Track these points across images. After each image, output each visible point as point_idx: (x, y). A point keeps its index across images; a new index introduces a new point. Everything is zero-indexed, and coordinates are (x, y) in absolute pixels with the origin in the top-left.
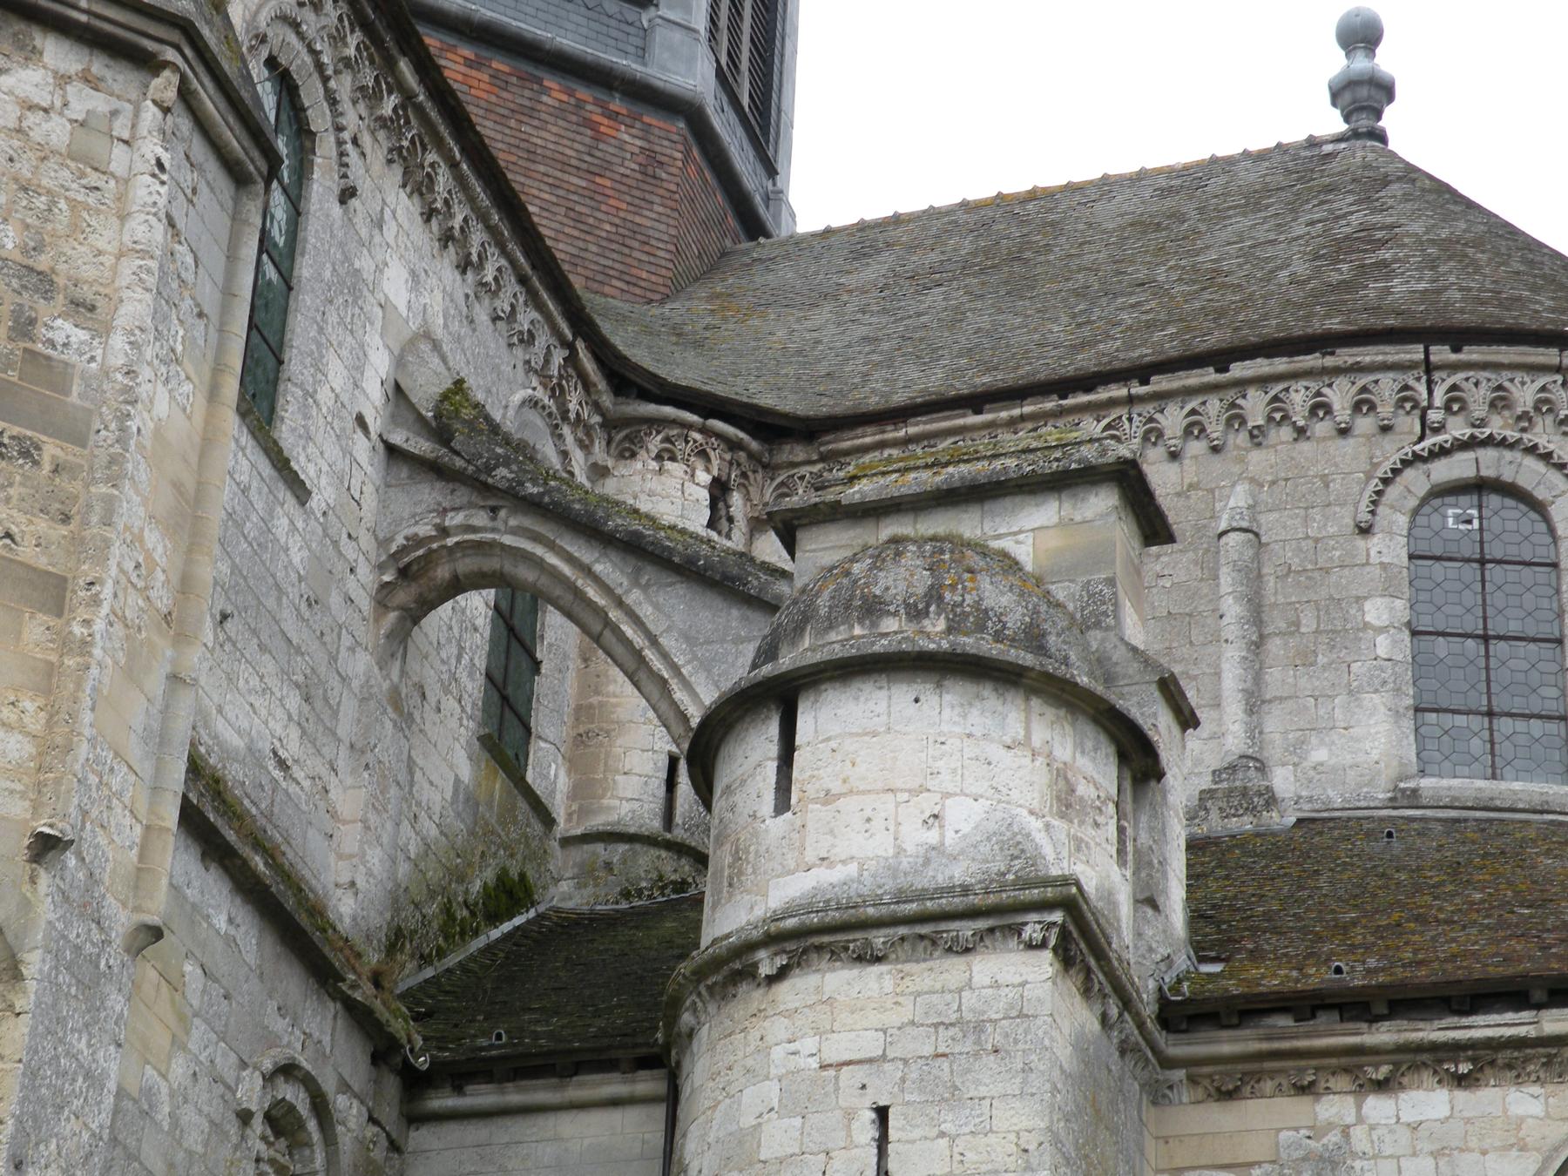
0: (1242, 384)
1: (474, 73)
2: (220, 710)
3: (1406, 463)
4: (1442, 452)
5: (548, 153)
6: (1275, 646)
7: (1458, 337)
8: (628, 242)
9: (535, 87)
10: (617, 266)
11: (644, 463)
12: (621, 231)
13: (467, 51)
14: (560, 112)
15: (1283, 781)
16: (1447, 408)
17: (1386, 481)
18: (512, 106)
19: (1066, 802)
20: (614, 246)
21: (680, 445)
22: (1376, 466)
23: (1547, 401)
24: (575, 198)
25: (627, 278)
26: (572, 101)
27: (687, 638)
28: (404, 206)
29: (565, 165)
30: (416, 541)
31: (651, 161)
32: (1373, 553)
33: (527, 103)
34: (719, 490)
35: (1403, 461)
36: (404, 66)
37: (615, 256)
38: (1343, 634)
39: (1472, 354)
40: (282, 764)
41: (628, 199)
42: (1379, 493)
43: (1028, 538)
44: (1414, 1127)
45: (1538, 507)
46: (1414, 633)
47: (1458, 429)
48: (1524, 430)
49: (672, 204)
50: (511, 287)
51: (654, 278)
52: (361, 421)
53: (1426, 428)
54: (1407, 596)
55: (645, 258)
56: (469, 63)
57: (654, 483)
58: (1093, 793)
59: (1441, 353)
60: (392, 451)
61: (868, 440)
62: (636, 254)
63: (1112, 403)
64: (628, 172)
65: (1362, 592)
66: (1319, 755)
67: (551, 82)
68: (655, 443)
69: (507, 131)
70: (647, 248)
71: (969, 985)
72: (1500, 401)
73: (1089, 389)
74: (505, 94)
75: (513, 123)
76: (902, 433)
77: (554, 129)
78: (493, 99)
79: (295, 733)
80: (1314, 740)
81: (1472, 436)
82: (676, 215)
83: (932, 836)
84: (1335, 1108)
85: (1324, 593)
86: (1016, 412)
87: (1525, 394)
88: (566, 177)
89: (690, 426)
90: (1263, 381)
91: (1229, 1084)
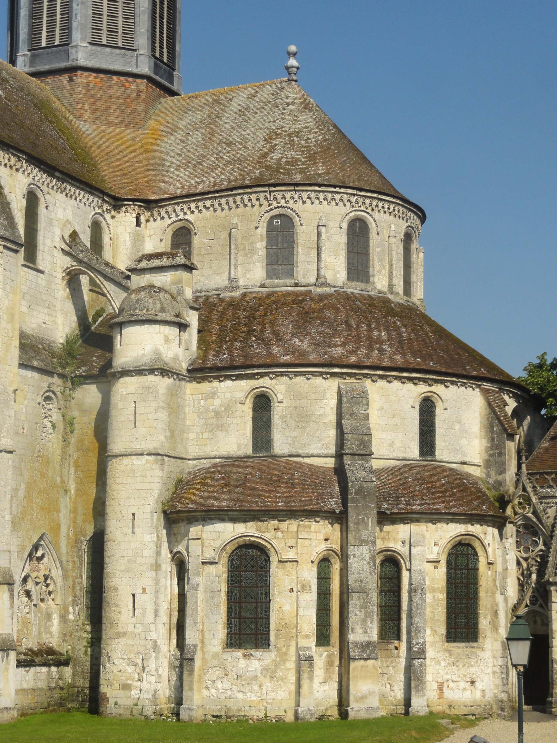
0: (236, 195)
1: (97, 80)
2: (31, 323)
4: (272, 210)
6: (241, 253)
7: (274, 185)
11: (122, 214)
13: (95, 75)
14: (117, 85)
15: (241, 282)
16: (273, 199)
17: (261, 217)
19: (167, 340)
21: (129, 209)
27: (113, 291)
28: (60, 197)
29: (118, 98)
30: (69, 268)
31: (139, 91)
34: (138, 219)
36: (57, 174)
38: (253, 251)
39: (277, 188)
40: (45, 323)
44: (227, 387)
45: (291, 219)
47: (275, 204)
50: (87, 195)
52: (55, 247)
53: (269, 205)
57: (124, 219)
58: (173, 337)
59: (272, 189)
60: (62, 249)
63: (212, 197)
65: (257, 241)
66: (248, 276)
67: (114, 77)
68: (124, 209)
71: (147, 381)
72: (284, 198)
75: (106, 90)
76: (173, 202)
77: (116, 89)
78: (101, 85)
79: (47, 316)
83: (143, 352)
84: (216, 384)
87: (288, 195)
89: (131, 205)
91: (199, 380)
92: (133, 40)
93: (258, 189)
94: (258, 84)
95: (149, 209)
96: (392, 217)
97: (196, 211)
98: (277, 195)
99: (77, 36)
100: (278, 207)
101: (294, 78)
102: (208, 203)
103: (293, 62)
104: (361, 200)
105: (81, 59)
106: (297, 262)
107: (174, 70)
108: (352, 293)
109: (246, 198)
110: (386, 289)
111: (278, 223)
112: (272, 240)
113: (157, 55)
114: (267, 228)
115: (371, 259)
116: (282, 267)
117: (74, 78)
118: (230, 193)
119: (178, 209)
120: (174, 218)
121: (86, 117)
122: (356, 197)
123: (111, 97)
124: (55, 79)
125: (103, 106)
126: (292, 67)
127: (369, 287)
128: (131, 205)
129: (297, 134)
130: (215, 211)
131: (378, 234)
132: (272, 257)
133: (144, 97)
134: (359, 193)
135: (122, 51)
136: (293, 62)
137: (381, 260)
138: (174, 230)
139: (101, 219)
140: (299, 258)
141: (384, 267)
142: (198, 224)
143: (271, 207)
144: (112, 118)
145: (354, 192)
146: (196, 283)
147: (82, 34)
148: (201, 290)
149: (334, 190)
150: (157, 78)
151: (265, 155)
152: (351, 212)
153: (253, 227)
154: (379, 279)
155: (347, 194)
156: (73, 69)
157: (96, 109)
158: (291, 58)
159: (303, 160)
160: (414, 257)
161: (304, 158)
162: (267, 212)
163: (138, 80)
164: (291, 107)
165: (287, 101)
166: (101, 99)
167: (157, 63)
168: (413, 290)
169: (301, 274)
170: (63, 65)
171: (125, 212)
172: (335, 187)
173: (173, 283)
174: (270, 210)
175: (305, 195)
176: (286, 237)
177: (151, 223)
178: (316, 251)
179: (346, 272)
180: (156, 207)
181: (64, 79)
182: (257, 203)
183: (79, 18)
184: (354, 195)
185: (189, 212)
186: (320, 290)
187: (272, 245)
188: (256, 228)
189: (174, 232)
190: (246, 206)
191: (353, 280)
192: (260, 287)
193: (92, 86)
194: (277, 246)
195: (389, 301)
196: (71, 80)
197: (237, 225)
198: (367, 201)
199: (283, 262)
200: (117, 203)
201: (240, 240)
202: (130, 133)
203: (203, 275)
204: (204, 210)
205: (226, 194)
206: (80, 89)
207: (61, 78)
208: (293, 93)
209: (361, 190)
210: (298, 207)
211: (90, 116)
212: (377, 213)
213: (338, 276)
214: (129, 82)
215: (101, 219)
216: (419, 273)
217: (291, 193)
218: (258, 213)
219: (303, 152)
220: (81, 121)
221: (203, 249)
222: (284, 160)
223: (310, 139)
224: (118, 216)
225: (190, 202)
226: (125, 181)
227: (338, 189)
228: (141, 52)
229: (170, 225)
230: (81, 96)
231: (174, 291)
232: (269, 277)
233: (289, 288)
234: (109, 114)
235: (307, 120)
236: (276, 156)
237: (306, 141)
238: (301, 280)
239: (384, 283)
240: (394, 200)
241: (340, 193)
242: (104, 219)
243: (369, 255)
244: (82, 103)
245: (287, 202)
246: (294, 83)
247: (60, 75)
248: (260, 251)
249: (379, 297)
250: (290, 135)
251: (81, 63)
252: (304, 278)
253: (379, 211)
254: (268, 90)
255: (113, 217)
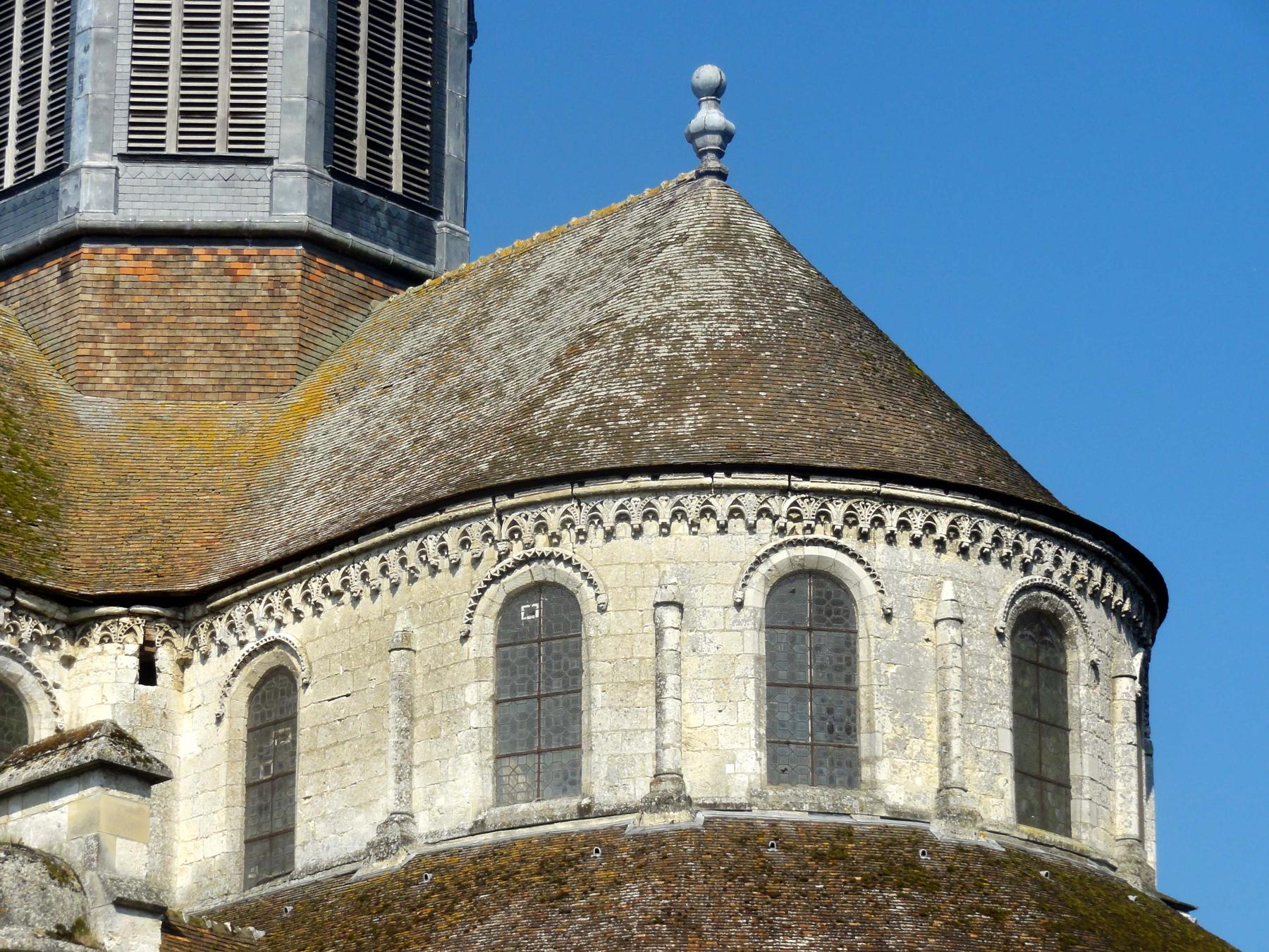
0: (404, 539)
1: (141, 264)
3: (488, 583)
4: (509, 571)
5: (199, 306)
6: (420, 728)
8: (262, 354)
9: (187, 257)
10: (256, 375)
11: (94, 647)
12: (257, 347)
13: (136, 249)
14: (206, 271)
15: (423, 825)
17: (477, 599)
18: (170, 279)
20: (252, 361)
22: (473, 586)
23: (569, 520)
24: (221, 333)
25: (263, 382)
26: (215, 258)
29: (211, 311)
31: (278, 282)
32: (471, 651)
33: (181, 272)
35: (485, 582)
37: (253, 368)
38: (454, 716)
39: (520, 498)
41: (261, 320)
42: (473, 608)
43: (66, 808)
45: (572, 595)
46: (498, 702)
47: (518, 552)
48: (556, 545)
49: (295, 313)
51: (283, 376)
54: (492, 675)
55: (275, 362)
56: (137, 258)
57: (99, 662)
59: (504, 502)
61: (228, 598)
62: (269, 362)
64: (260, 299)
66: (440, 802)
67: (198, 250)
68: (97, 632)
69: (168, 300)
70: (277, 354)
72: (541, 527)
73: (331, 550)
74: (165, 272)
75: (171, 292)
78: (156, 278)
80: (438, 792)
81: (525, 556)
82: (298, 320)
85: (447, 682)
86: (297, 570)
87: (553, 518)
88: (212, 320)
89: (120, 615)
90: (414, 534)
92: (258, 131)
93: (462, 510)
94: (620, 204)
95: (184, 624)
96: (950, 557)
97: (307, 611)
98: (521, 520)
99: (81, 139)
100: (527, 561)
101: (712, 163)
102: (335, 579)
103: (710, 115)
104: (809, 509)
105: (88, 206)
106: (590, 735)
107: (436, 214)
108: (773, 824)
109: (431, 543)
110: (927, 804)
111: (531, 612)
112: (514, 673)
113: (360, 172)
114: (500, 635)
115: (863, 702)
116: (547, 759)
117: (73, 267)
118: (388, 535)
119: (258, 609)
120: (253, 642)
121: (107, 380)
122: (793, 498)
123: (187, 312)
124: (29, 280)
125: (161, 340)
126: (705, 131)
127: (850, 800)
128: (120, 615)
129: (653, 329)
130: (356, 600)
131: (888, 617)
132: (513, 729)
133: (294, 299)
134: (799, 483)
135: (226, 170)
136: (710, 115)
137: (905, 706)
138: (255, 681)
139: (15, 668)
140: (595, 720)
141: (919, 732)
142: (313, 653)
143: (505, 562)
144: (190, 374)
145: (782, 480)
146: (305, 843)
147: (95, 133)
148: (315, 867)
149: (708, 480)
150: (349, 238)
151: (537, 403)
152: (774, 550)
153: (454, 636)
154: (896, 770)
155: (756, 489)
156: (68, 242)
157: (138, 353)
158: (704, 105)
159: (641, 402)
160: (1080, 693)
161: (646, 396)
162: (495, 579)
163: (274, 251)
164: (673, 250)
165: (665, 236)
166: (155, 320)
167: (349, 193)
168: (1081, 807)
169: (603, 774)
170: (41, 234)
171: (102, 641)
172: (708, 469)
173: (77, 831)
174: (503, 575)
175: (609, 510)
176: (558, 657)
177: (196, 671)
178: (652, 693)
179: (763, 755)
180: (205, 616)
181: (48, 273)
182: (467, 557)
183: (88, 88)
184: (785, 491)
185: (288, 618)
186: (653, 822)
187: (513, 691)
188: (465, 637)
189: (257, 689)
190: (434, 570)
191: (792, 782)
192: (472, 833)
193: (127, 285)
194: (530, 689)
195: (919, 839)
196: (65, 275)
197: (407, 635)
198: (837, 510)
199: (549, 741)
200: (74, 615)
201: (419, 687)
202: (247, 411)
203: (323, 816)
204: (327, 604)
205: (377, 539)
206: (89, 297)
207: (43, 273)
208: (699, 209)
209: (806, 471)
210: (592, 552)
211: (119, 374)
212: (882, 545)
213: (729, 769)
214: (245, 259)
215: (15, 668)
216: (1119, 750)
217: (565, 507)
218: (468, 587)
219: (649, 379)
220: (89, 392)
221: (323, 730)
222: (576, 413)
223: (690, 338)
224: (81, 654)
225: (289, 582)
226: (135, 546)
227: (720, 478)
228: (286, 163)
229: (239, 667)
230: (90, 318)
231: (74, 854)
232: (502, 795)
233: (561, 827)
234: (180, 363)
235: (712, 281)
236: (560, 403)
237: (675, 346)
238: (603, 796)
239: (919, 781)
240: (948, 499)
241: (729, 489)
242: (29, 666)
243: (856, 690)
244: (95, 340)
245: (555, 539)
246: (709, 181)
247: (41, 266)
248: (474, 714)
249: (883, 830)
250: (629, 335)
251: (87, 217)
252: (612, 787)
253: (891, 539)
254: (638, 214)
255: (68, 662)
